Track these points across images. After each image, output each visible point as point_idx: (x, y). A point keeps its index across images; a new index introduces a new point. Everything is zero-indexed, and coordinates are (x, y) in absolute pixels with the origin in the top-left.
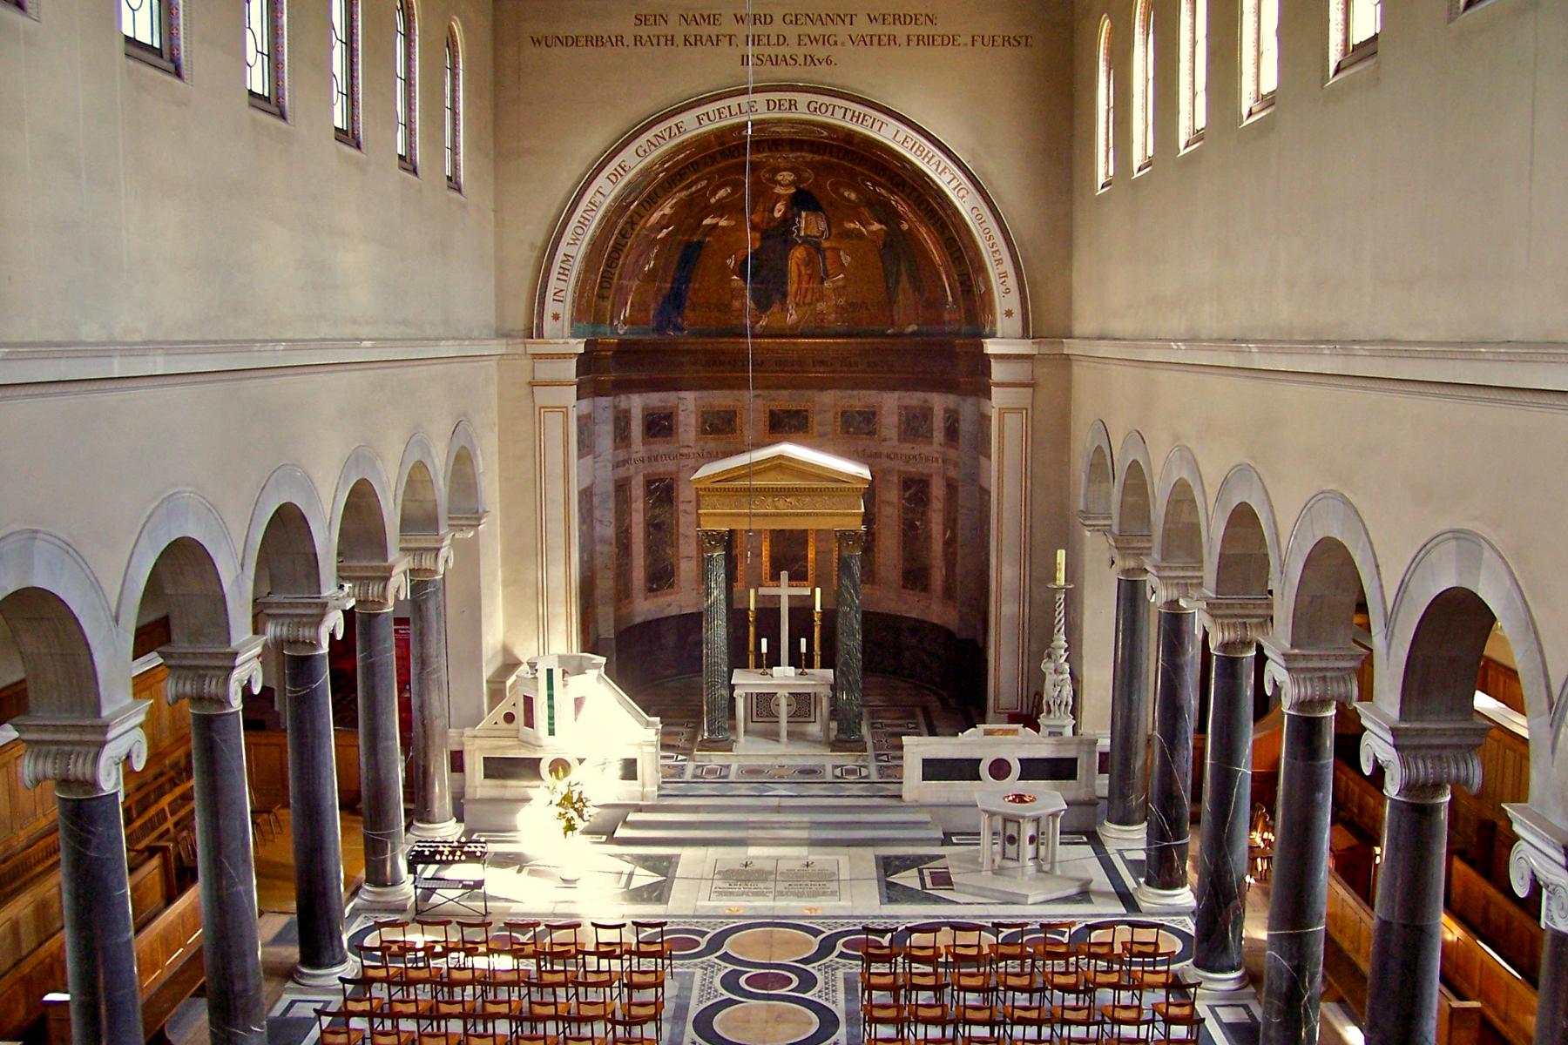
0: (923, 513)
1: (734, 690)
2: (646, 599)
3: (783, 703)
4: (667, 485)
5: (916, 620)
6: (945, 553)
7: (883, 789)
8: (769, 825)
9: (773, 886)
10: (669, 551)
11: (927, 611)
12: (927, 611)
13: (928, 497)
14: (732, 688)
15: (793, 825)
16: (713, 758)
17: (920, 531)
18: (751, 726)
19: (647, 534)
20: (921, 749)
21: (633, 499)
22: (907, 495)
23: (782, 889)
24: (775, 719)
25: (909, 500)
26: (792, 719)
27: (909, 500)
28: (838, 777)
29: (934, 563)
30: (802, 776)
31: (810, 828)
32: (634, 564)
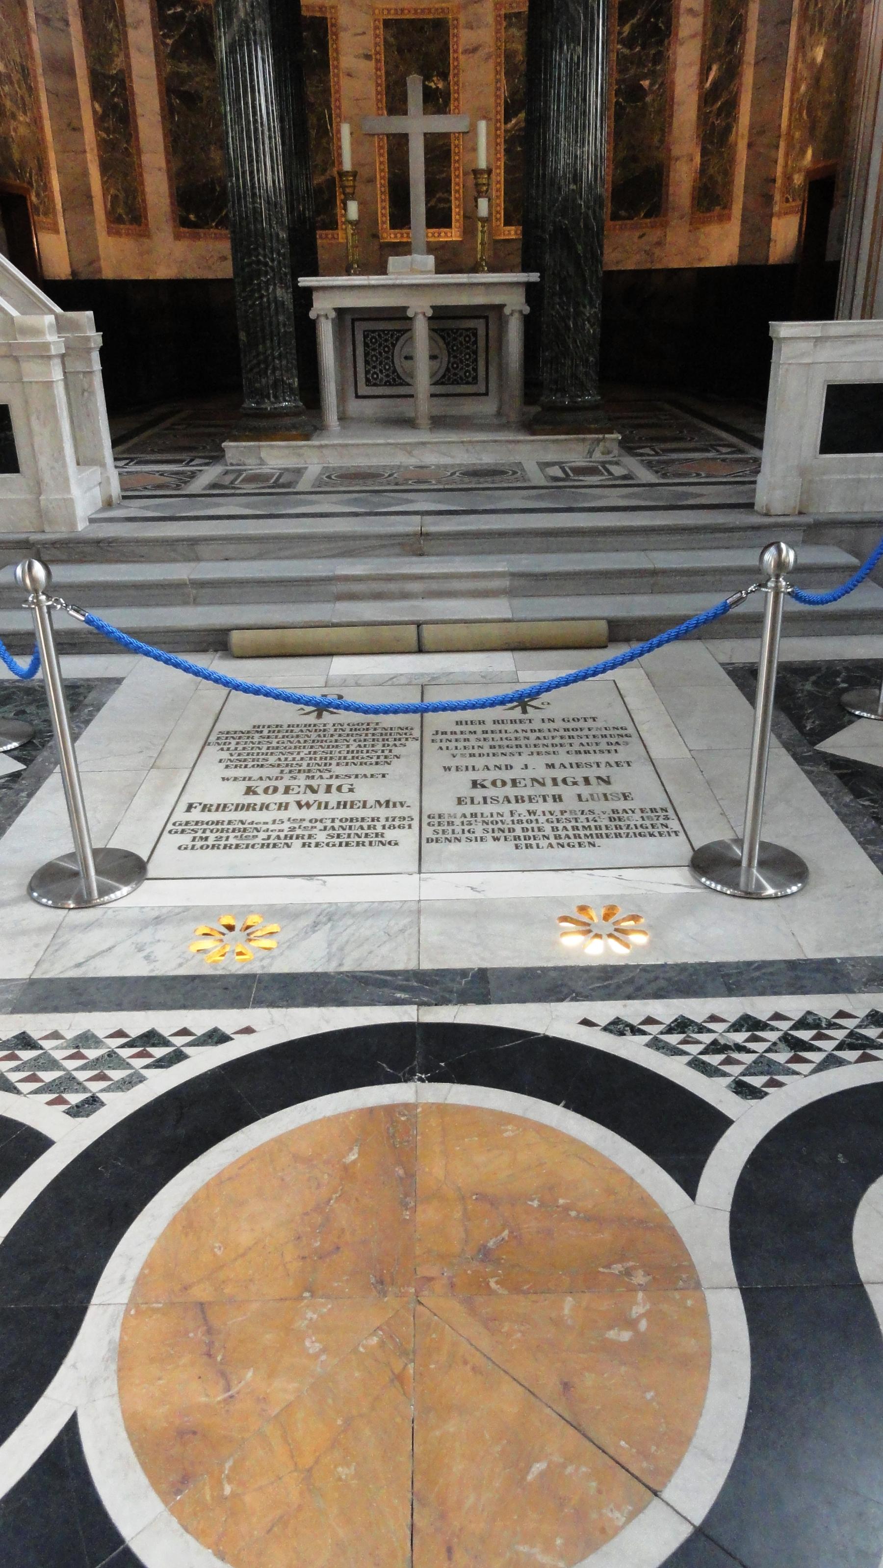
0: (659, 58)
1: (310, 305)
2: (178, 237)
3: (421, 329)
4: (198, 16)
5: (635, 273)
6: (703, 119)
7: (686, 495)
8: (392, 587)
9: (410, 795)
10: (216, 155)
11: (657, 251)
12: (657, 251)
13: (669, 24)
14: (305, 297)
15: (456, 585)
16: (263, 454)
17: (648, 99)
18: (354, 406)
19: (168, 111)
20: (825, 354)
21: (129, 20)
22: (627, 29)
23: (447, 806)
24: (402, 390)
25: (629, 43)
26: (439, 389)
27: (629, 43)
28: (556, 479)
29: (676, 151)
30: (466, 479)
31: (509, 593)
32: (146, 158)
